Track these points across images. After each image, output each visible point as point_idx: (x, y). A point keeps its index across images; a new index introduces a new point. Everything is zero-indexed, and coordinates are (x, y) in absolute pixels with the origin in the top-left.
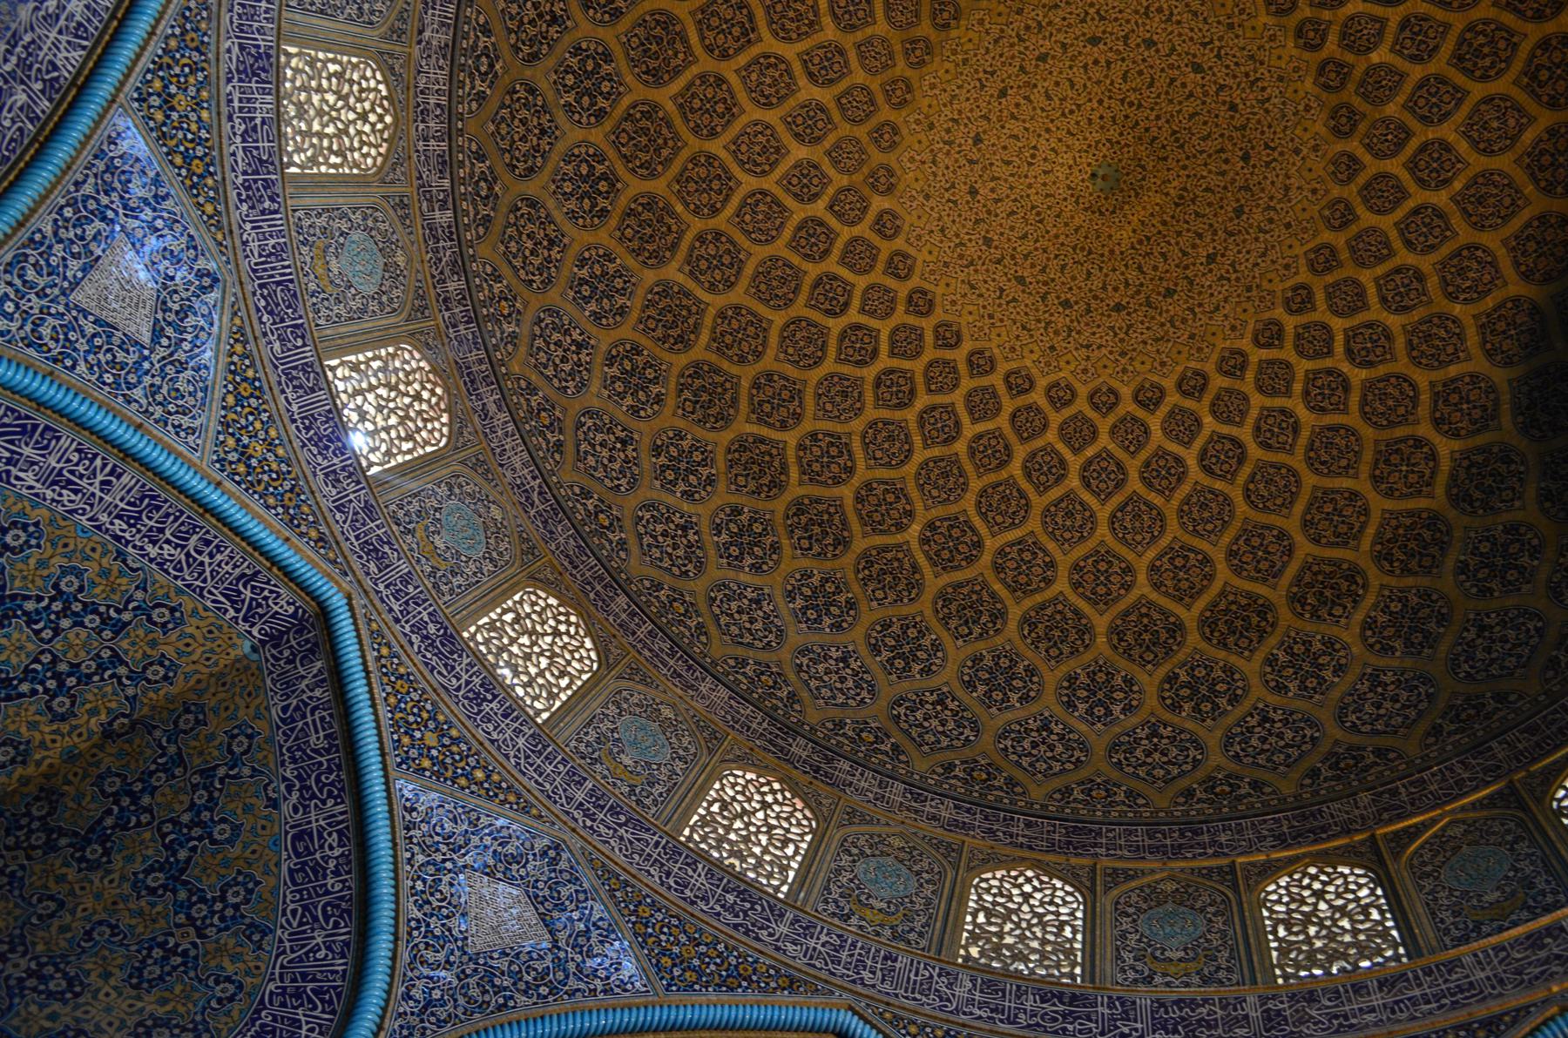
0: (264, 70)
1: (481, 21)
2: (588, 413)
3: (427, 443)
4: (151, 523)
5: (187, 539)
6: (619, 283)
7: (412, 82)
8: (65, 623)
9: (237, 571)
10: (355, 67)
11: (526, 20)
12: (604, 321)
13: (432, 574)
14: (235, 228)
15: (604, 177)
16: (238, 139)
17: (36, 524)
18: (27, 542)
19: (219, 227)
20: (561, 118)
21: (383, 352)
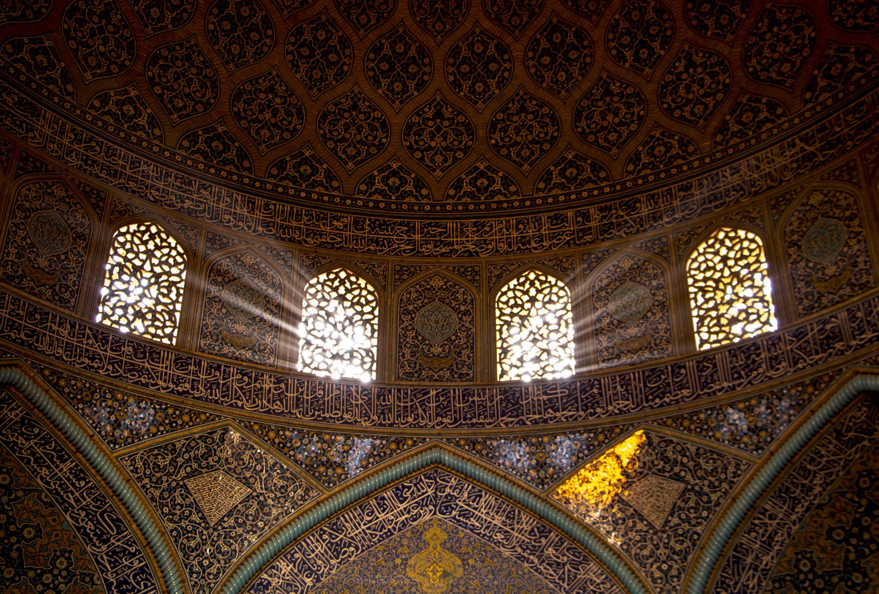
0: (514, 395)
1: (452, 192)
2: (746, 59)
3: (757, 261)
4: (798, 491)
5: (810, 471)
6: (635, 16)
7: (505, 257)
8: (866, 536)
9: (834, 441)
10: (502, 314)
11: (444, 144)
12: (669, 33)
13: (852, 285)
14: (612, 419)
15: (549, 39)
16: (558, 414)
17: (797, 554)
18: (808, 559)
19: (611, 431)
20: (510, 90)
21: (692, 289)
